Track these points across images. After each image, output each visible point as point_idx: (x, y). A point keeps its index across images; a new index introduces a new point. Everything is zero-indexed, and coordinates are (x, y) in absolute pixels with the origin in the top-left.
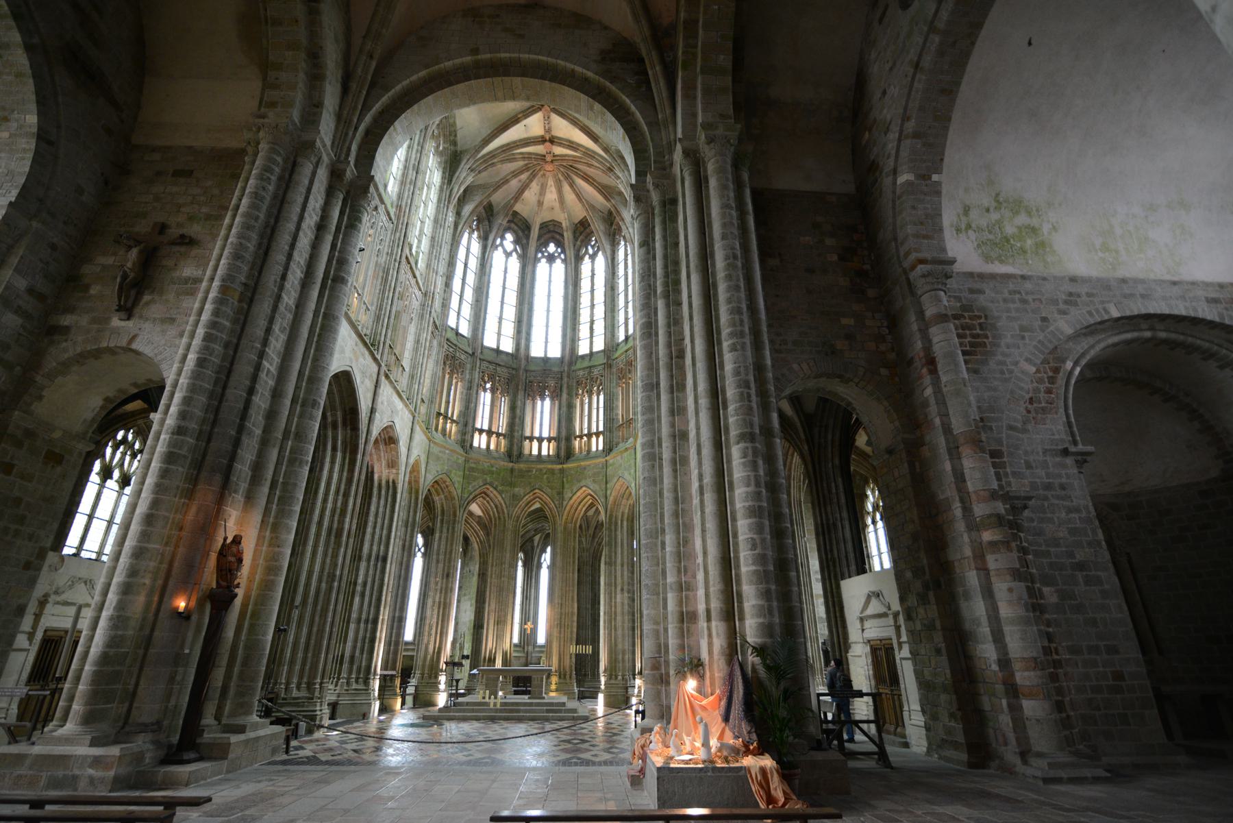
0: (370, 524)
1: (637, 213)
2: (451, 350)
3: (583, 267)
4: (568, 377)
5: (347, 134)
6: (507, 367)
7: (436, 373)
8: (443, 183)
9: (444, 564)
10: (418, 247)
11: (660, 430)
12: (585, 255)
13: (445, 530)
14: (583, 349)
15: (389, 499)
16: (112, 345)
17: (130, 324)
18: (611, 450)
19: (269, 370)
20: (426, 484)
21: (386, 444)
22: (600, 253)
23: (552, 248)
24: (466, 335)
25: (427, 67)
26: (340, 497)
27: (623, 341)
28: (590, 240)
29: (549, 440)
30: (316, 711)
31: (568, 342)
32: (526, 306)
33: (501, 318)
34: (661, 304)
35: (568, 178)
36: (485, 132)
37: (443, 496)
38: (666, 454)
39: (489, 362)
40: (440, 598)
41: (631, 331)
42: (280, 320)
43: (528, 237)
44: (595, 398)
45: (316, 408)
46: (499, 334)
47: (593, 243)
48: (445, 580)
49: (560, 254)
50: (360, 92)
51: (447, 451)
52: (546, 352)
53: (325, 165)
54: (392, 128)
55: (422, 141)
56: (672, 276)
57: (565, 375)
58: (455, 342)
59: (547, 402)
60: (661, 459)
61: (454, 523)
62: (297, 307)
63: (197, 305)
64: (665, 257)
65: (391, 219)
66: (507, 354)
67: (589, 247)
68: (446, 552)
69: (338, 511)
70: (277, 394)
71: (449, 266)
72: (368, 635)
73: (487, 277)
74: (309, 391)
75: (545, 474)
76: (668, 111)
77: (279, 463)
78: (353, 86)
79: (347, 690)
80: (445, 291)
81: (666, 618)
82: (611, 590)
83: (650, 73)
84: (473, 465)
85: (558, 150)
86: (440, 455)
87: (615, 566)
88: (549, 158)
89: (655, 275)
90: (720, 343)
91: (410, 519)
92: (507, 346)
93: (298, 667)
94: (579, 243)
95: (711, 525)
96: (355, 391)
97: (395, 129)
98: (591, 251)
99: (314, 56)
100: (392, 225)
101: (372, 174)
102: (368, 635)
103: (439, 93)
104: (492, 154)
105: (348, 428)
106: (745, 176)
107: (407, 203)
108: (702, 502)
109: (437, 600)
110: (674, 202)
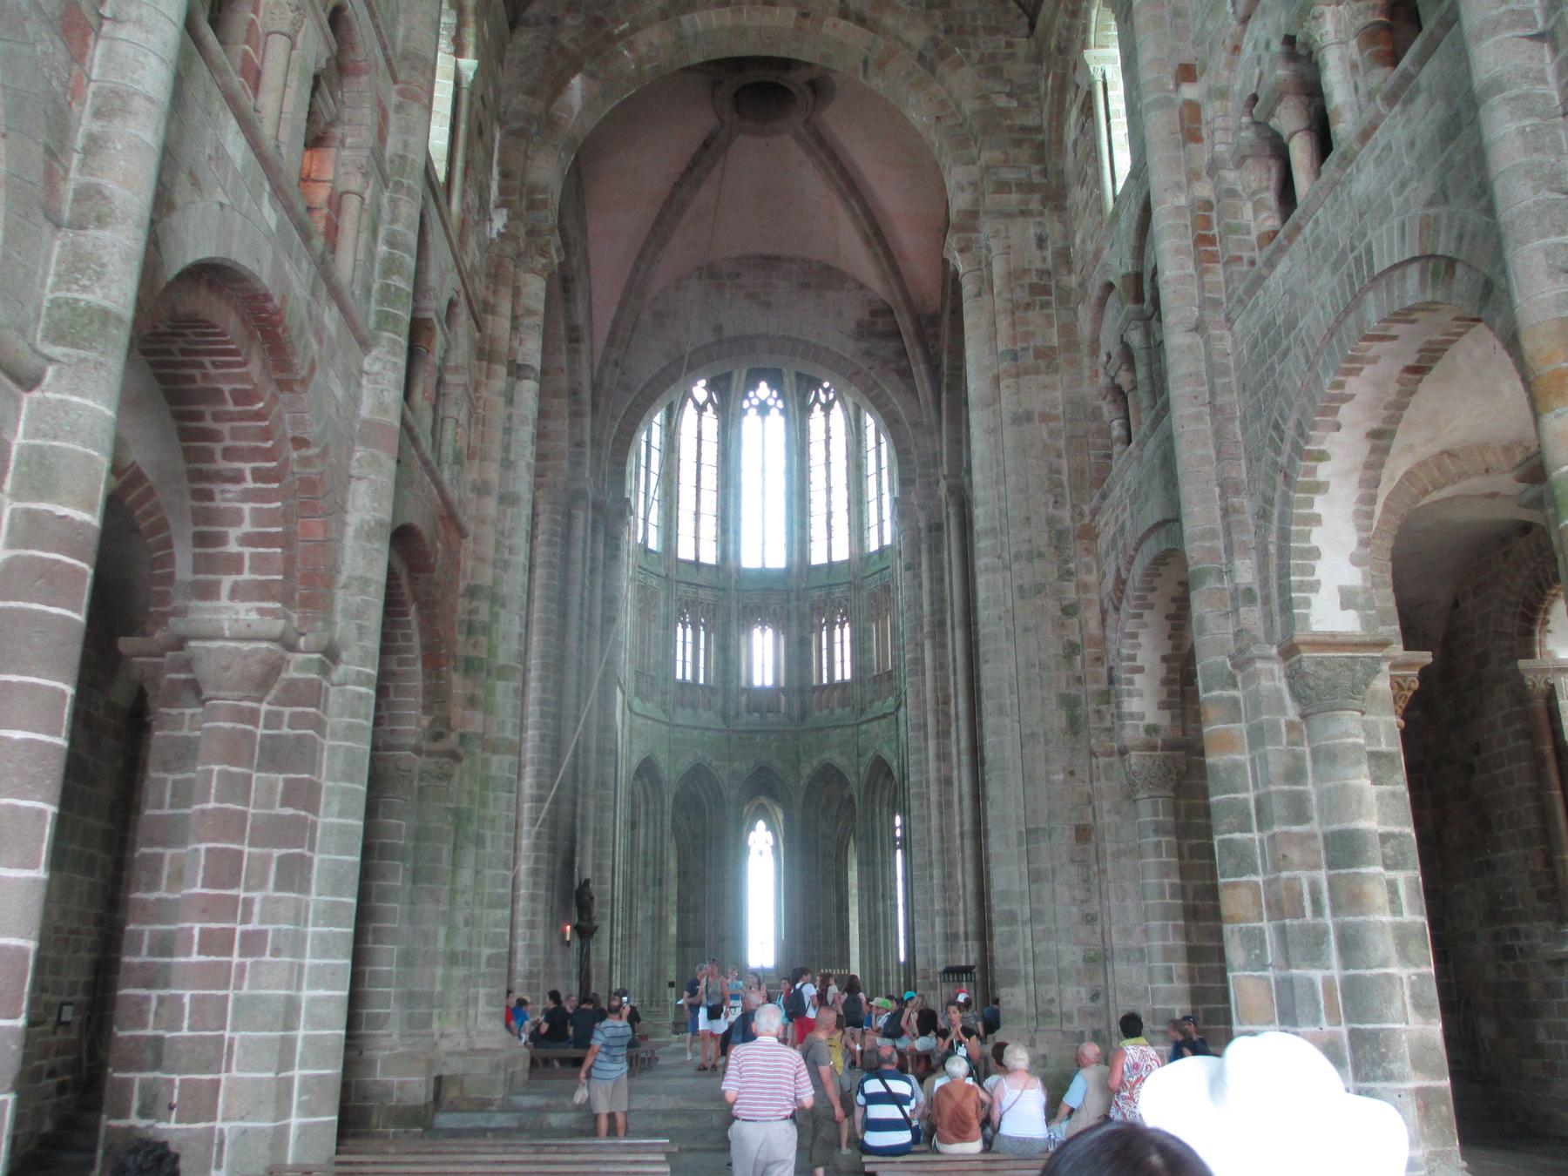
3: (812, 422)
6: (712, 588)
11: (927, 772)
13: (651, 824)
18: (862, 711)
22: (837, 404)
23: (763, 390)
24: (655, 549)
27: (875, 552)
31: (796, 546)
33: (697, 514)
34: (928, 645)
38: (934, 797)
39: (689, 584)
41: (887, 541)
44: (837, 631)
46: (697, 538)
57: (793, 596)
59: (769, 632)
64: (932, 592)
66: (710, 567)
67: (821, 391)
76: (934, 418)
81: (933, 937)
84: (679, 735)
89: (921, 606)
92: (709, 556)
95: (969, 866)
98: (823, 398)
99: (574, 393)
108: (962, 844)
109: (650, 913)
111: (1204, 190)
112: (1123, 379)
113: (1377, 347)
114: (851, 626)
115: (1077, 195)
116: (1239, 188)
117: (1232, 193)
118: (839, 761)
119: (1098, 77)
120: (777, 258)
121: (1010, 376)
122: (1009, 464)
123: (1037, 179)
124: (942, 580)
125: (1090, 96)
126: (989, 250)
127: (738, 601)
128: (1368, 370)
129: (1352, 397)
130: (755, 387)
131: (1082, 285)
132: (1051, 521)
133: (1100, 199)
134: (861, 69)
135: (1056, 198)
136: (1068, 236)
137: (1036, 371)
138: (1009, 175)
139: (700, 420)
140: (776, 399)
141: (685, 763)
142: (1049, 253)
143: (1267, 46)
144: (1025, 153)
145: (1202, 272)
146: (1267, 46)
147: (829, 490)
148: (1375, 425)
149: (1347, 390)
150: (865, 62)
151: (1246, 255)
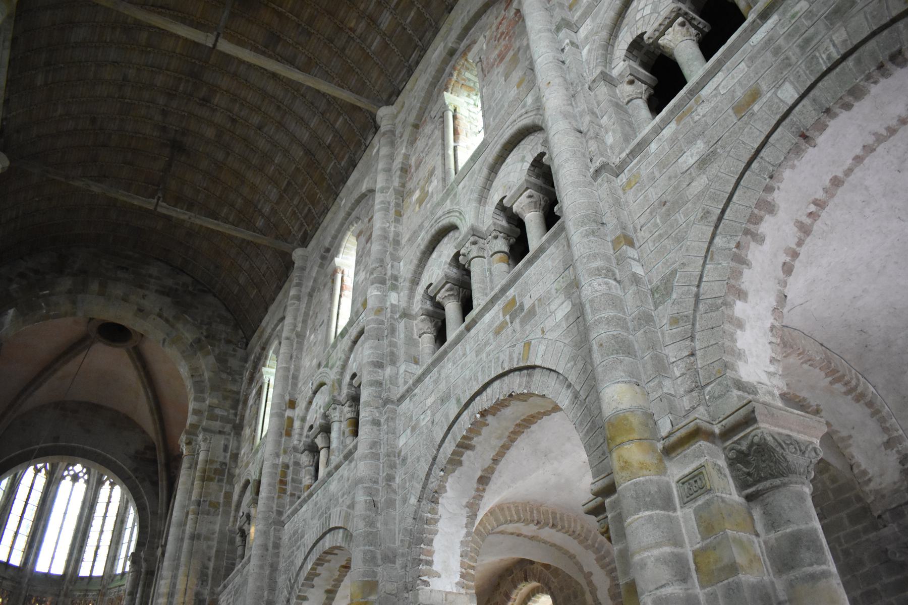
4: (66, 595)
12: (106, 480)
14: (84, 571)
23: (78, 468)
27: (119, 574)
32: (42, 523)
33: (16, 533)
41: (127, 569)
52: (50, 567)
66: (15, 567)
76: (164, 511)
111: (288, 459)
112: (245, 527)
113: (329, 557)
115: (247, 431)
116: (301, 462)
117: (297, 463)
119: (266, 381)
121: (194, 514)
122: (183, 559)
123: (232, 417)
125: (261, 388)
126: (199, 446)
127: (27, 592)
128: (326, 564)
129: (320, 574)
130: (74, 465)
131: (239, 475)
132: (197, 594)
133: (254, 438)
134: (162, 342)
135: (238, 429)
136: (239, 448)
137: (208, 514)
138: (218, 412)
139: (35, 477)
140: (85, 474)
142: (228, 455)
143: (320, 408)
144: (228, 403)
145: (279, 497)
146: (320, 408)
147: (102, 532)
148: (329, 587)
149: (317, 572)
150: (164, 340)
151: (297, 493)
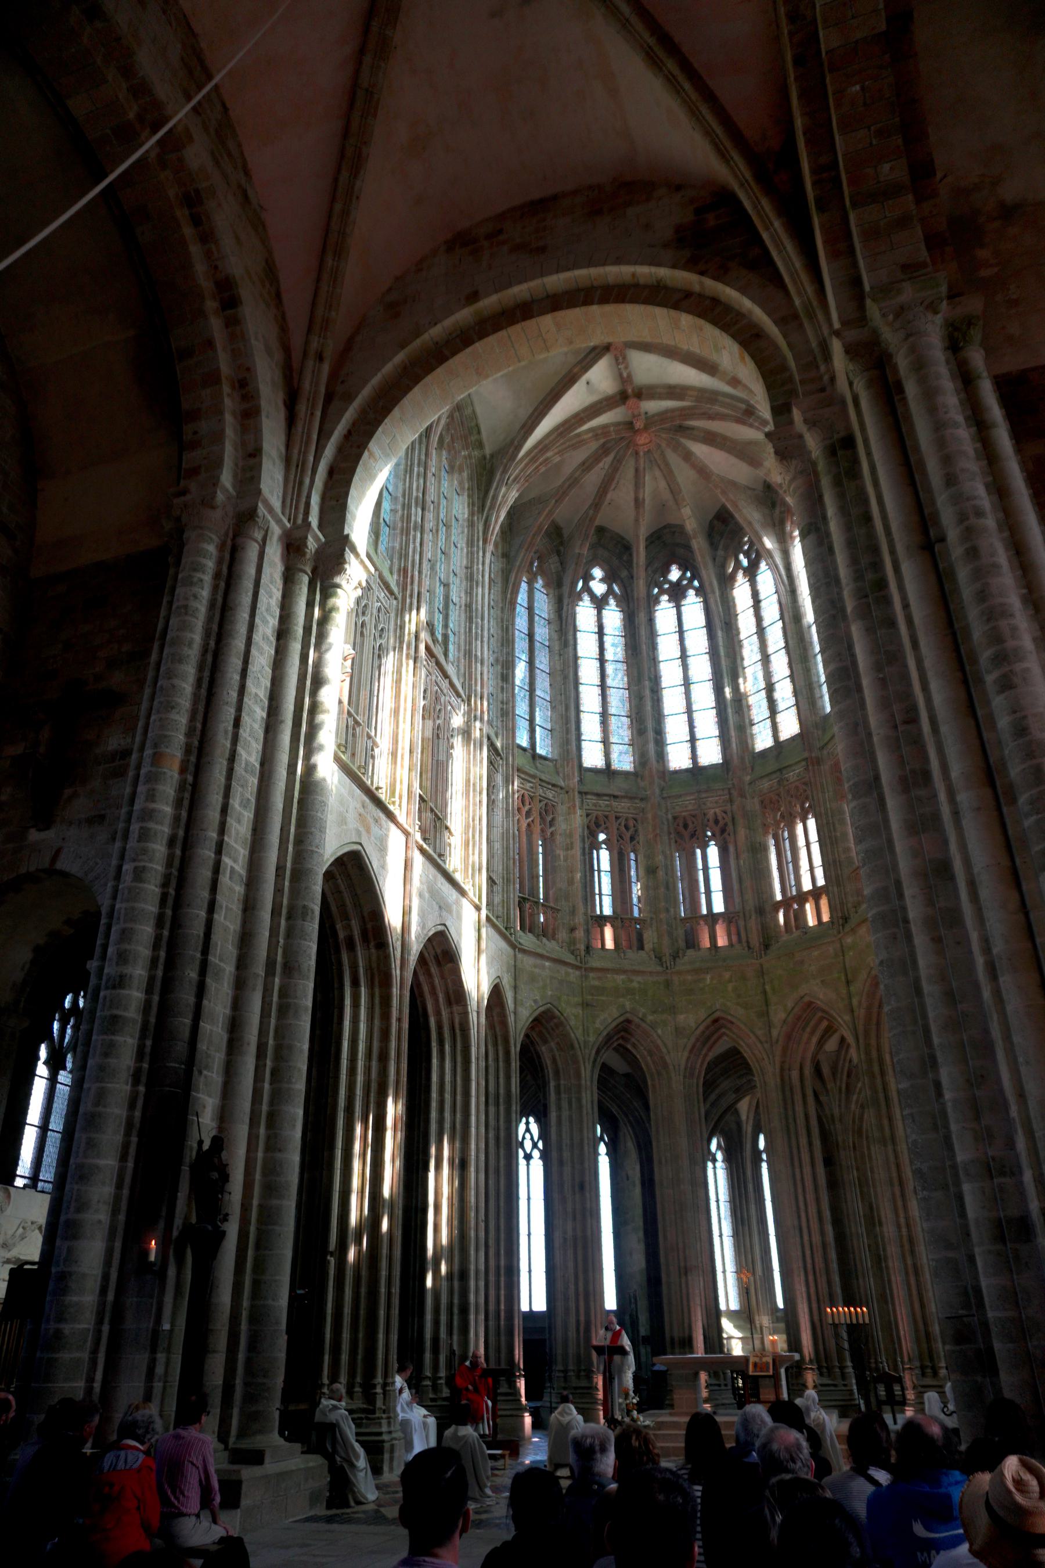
0: (434, 1105)
1: (788, 478)
2: (528, 785)
5: (301, 483)
6: (631, 798)
7: (508, 830)
8: (472, 514)
9: (573, 1167)
10: (446, 626)
13: (565, 1105)
14: (763, 740)
15: (459, 1059)
16: (32, 869)
17: (50, 834)
18: (846, 919)
19: (233, 870)
20: (519, 1027)
21: (439, 964)
22: (763, 565)
23: (675, 574)
24: (550, 756)
25: (402, 347)
26: (374, 1063)
28: (741, 544)
29: (727, 916)
30: (380, 1434)
33: (605, 716)
34: (856, 630)
35: (677, 447)
36: (524, 413)
37: (553, 1045)
38: (915, 911)
39: (598, 795)
40: (574, 1229)
42: (240, 789)
43: (629, 565)
44: (799, 828)
45: (308, 918)
47: (746, 547)
48: (577, 1196)
49: (691, 580)
50: (312, 414)
51: (547, 964)
53: (275, 538)
54: (366, 454)
55: (423, 457)
56: (870, 576)
57: (735, 793)
58: (533, 771)
60: (906, 921)
61: (579, 1092)
62: (262, 764)
63: (128, 790)
64: (851, 544)
65: (392, 593)
66: (626, 774)
67: (741, 556)
68: (572, 1145)
69: (374, 1086)
70: (249, 906)
71: (502, 645)
72: (456, 1301)
73: (571, 648)
74: (295, 893)
75: (730, 981)
76: (810, 289)
77: (265, 1014)
78: (302, 408)
79: (432, 1400)
80: (502, 688)
82: (893, 1194)
83: (765, 236)
84: (596, 983)
85: (652, 406)
86: (537, 970)
87: (894, 1143)
88: (639, 425)
89: (837, 581)
90: (980, 681)
91: (502, 1091)
92: (623, 761)
93: (345, 1357)
94: (721, 552)
96: (371, 879)
97: (371, 455)
98: (745, 562)
100: (395, 602)
101: (346, 533)
102: (456, 1301)
103: (428, 379)
104: (543, 446)
105: (372, 944)
106: (977, 358)
107: (413, 561)
108: (997, 993)
109: (570, 1233)
110: (848, 442)
114: (815, 816)
118: (821, 994)
120: (555, 198)
124: (867, 518)
127: (666, 813)
141: (606, 1018)
